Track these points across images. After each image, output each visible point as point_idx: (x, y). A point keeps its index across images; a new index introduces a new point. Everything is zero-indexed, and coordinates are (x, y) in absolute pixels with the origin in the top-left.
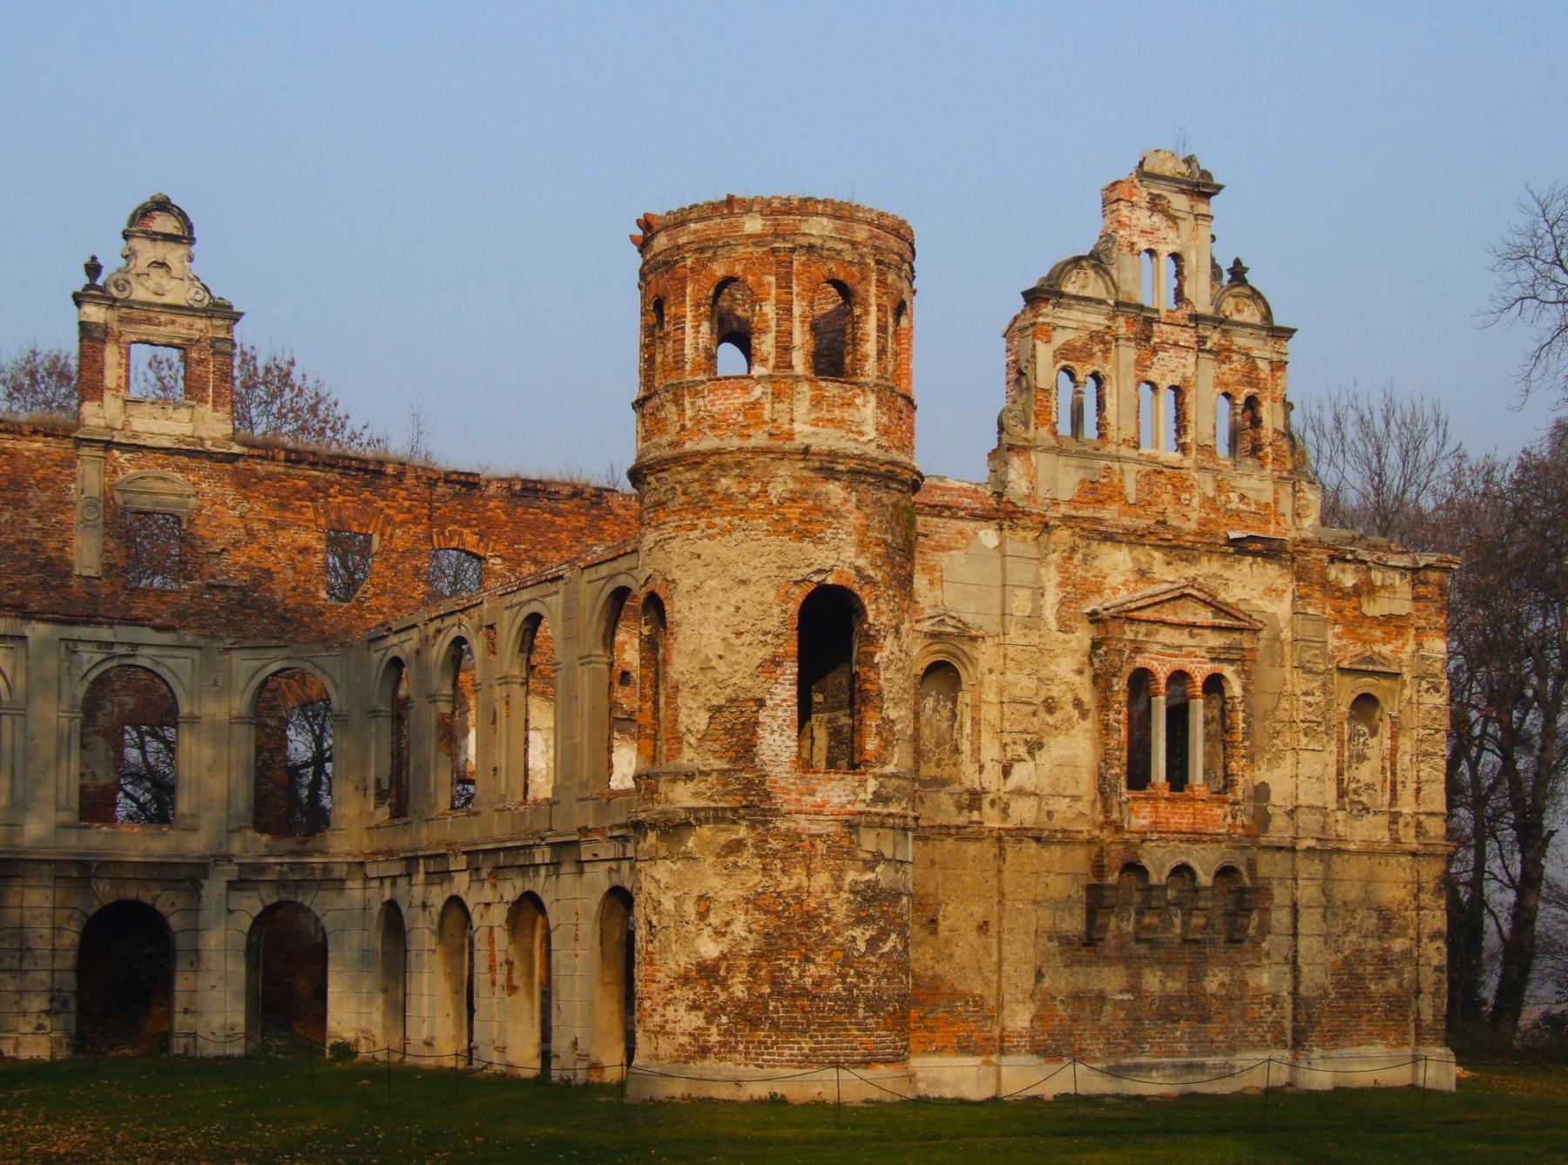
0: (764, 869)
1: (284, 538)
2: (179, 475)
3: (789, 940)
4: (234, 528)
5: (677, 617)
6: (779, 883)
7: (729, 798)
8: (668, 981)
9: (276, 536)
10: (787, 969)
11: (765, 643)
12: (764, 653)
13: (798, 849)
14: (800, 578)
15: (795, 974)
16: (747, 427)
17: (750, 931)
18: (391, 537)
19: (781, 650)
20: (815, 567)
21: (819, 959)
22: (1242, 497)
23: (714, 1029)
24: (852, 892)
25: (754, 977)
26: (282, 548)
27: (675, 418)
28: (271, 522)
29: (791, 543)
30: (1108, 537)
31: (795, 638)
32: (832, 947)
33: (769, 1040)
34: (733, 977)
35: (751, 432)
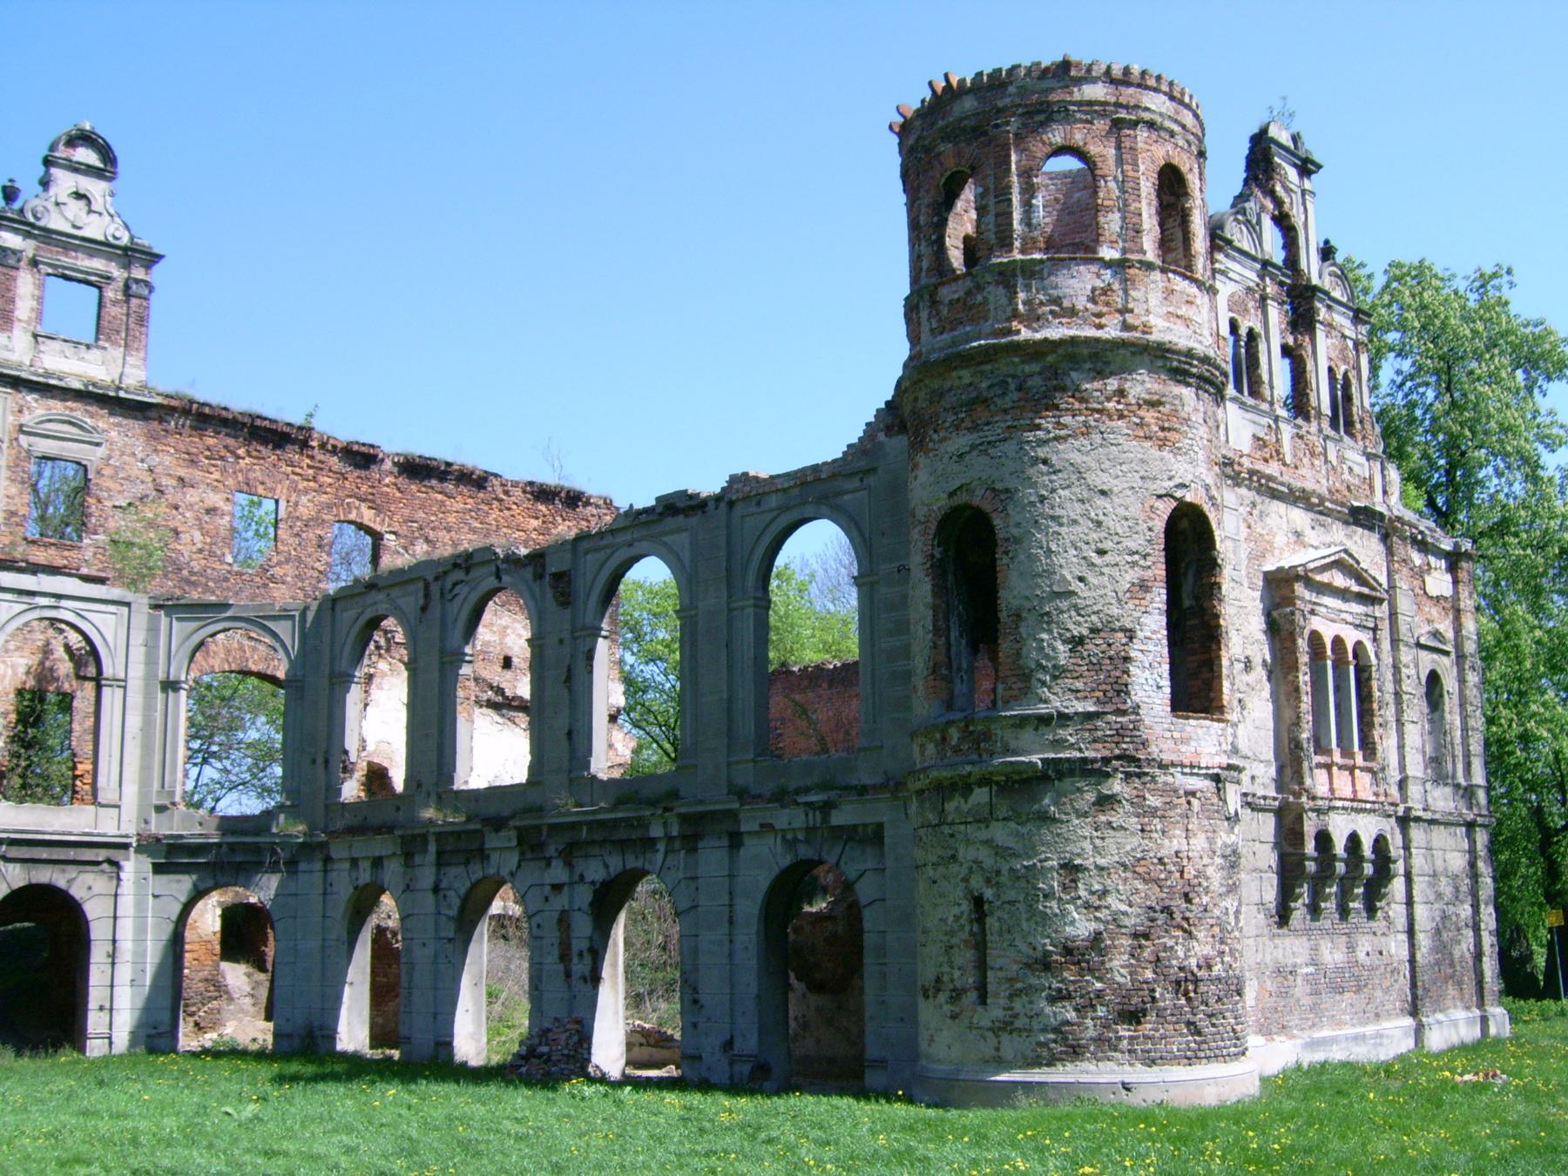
0: (1142, 830)
1: (192, 496)
2: (88, 420)
3: (1171, 914)
4: (142, 482)
5: (1015, 532)
6: (1160, 846)
7: (1100, 746)
8: (1015, 967)
9: (184, 494)
10: (1172, 947)
11: (1134, 564)
12: (1132, 576)
13: (1175, 806)
14: (1163, 492)
15: (1181, 954)
16: (1099, 315)
17: (1130, 906)
18: (296, 504)
19: (1149, 573)
20: (1177, 481)
21: (1201, 935)
22: (1350, 469)
23: (1089, 1022)
24: (1224, 857)
25: (1138, 960)
26: (190, 506)
27: (1004, 301)
28: (181, 479)
29: (1152, 451)
30: (1275, 495)
31: (1163, 560)
32: (1211, 921)
33: (1157, 1035)
34: (1111, 960)
35: (1103, 321)
